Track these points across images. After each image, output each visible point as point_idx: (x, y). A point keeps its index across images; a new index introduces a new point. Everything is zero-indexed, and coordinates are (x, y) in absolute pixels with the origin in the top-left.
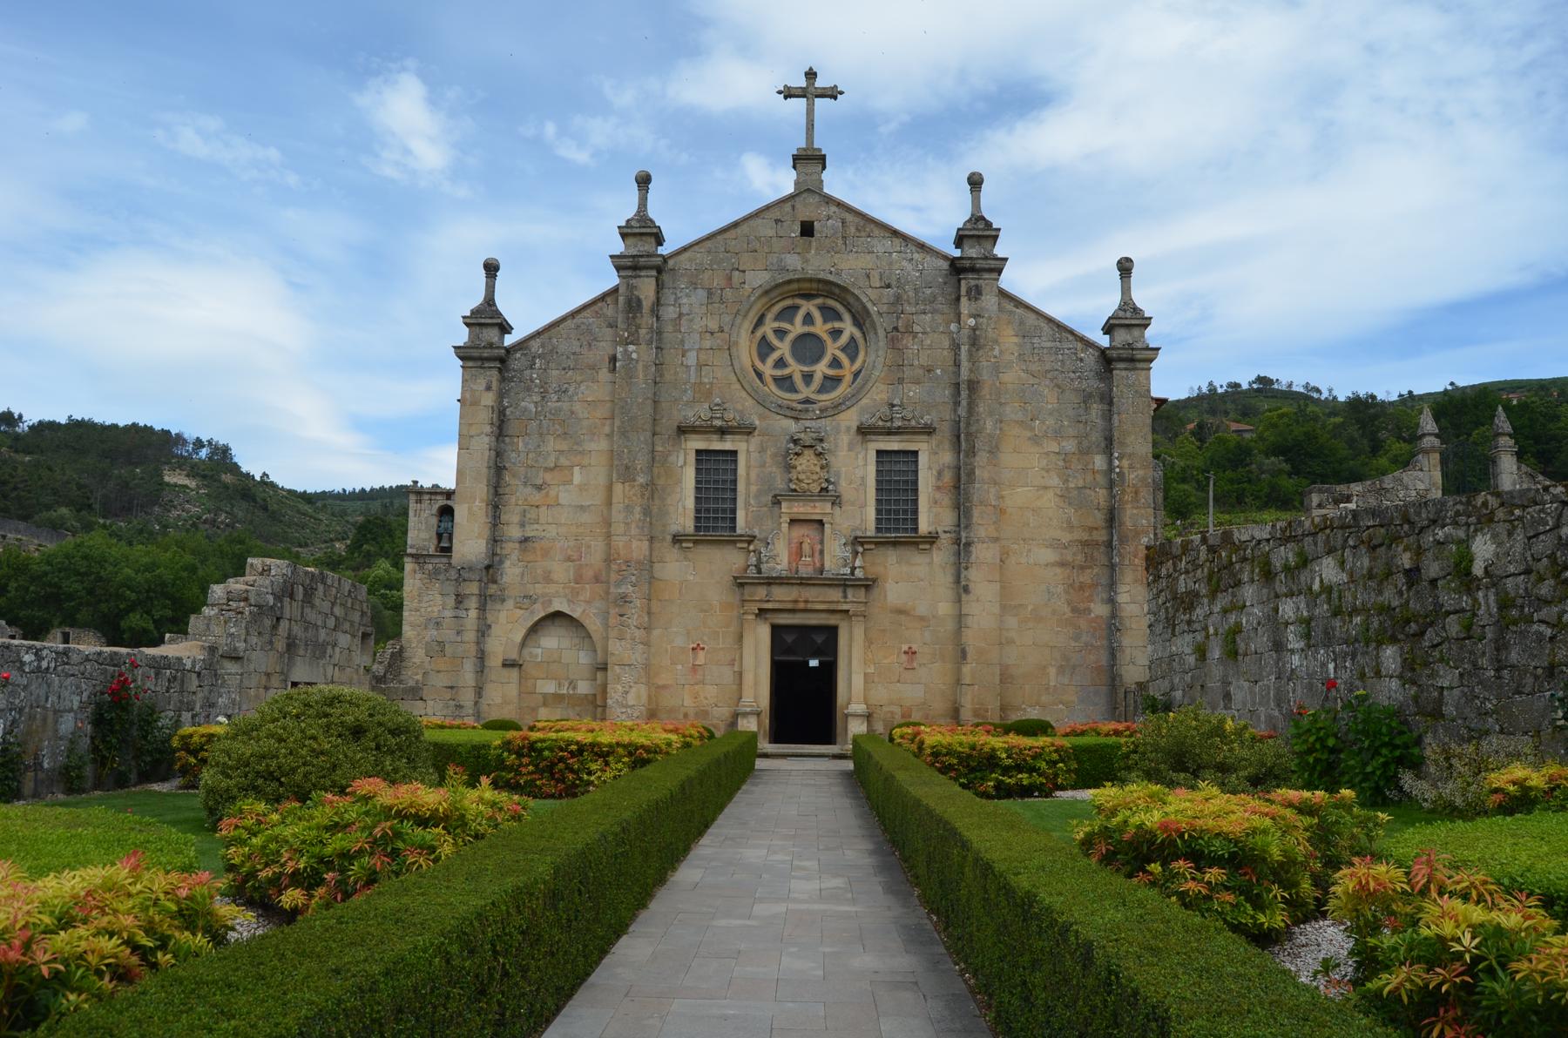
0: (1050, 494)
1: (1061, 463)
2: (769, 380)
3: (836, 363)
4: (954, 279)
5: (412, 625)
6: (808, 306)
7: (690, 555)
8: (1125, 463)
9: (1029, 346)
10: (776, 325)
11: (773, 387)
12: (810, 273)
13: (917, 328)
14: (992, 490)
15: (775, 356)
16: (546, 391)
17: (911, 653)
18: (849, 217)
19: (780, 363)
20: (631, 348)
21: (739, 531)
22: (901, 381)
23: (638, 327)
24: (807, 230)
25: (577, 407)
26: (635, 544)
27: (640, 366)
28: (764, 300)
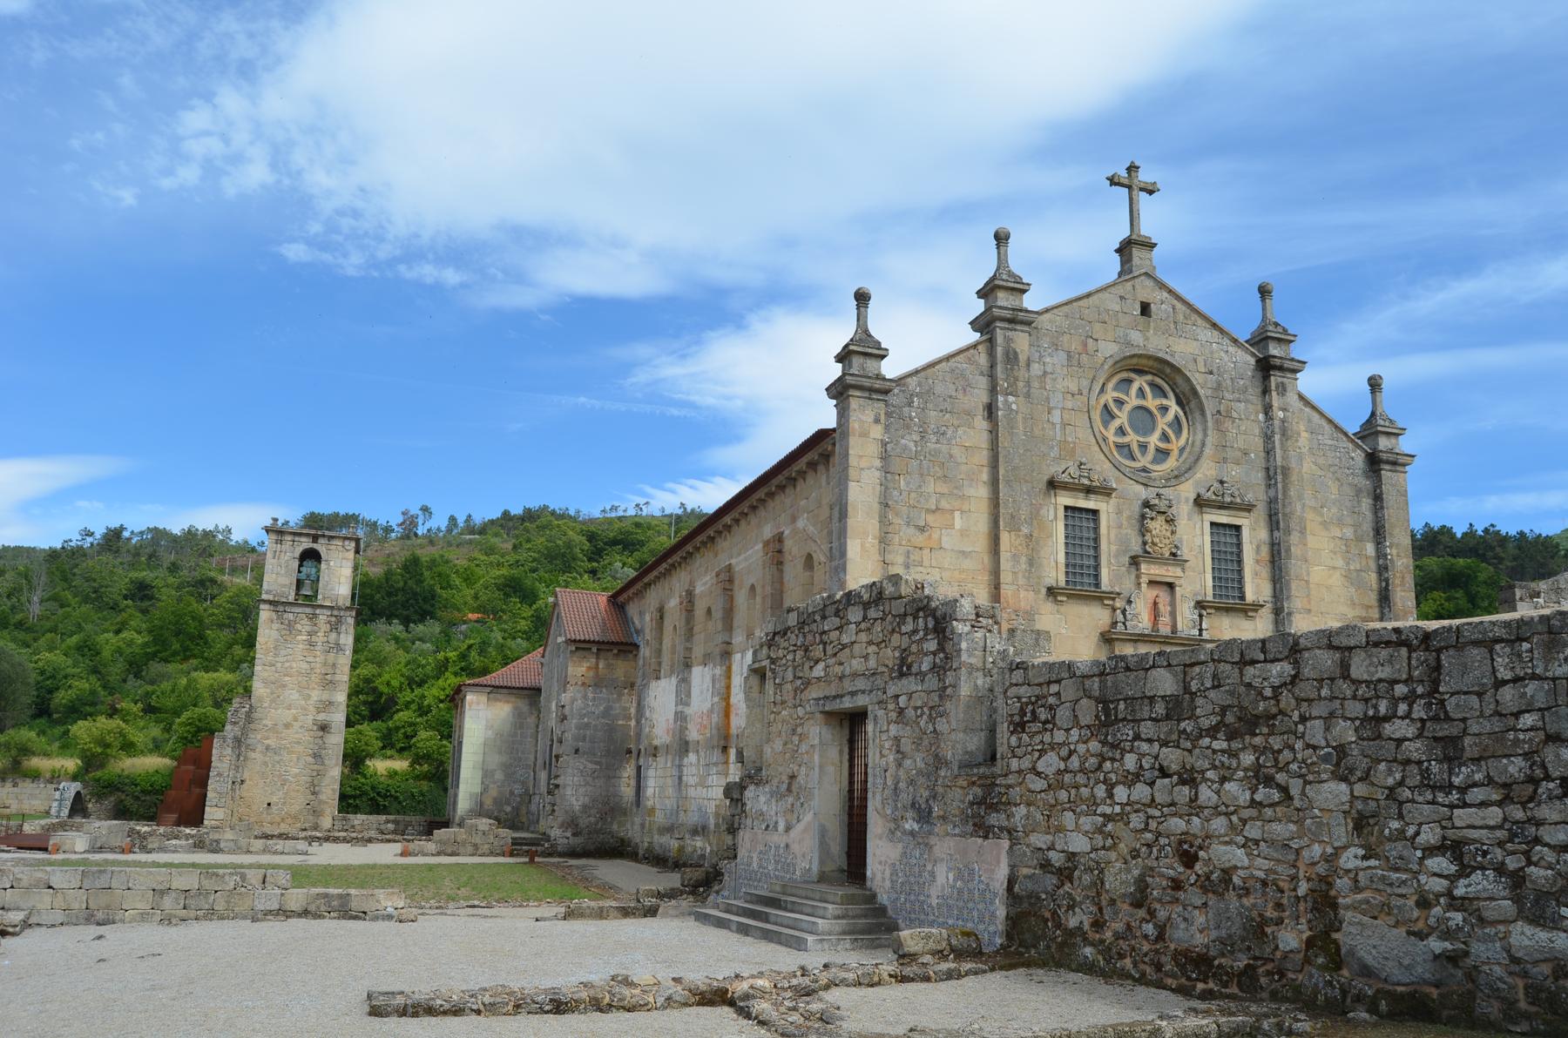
0: (1337, 574)
3: (1165, 437)
5: (265, 681)
6: (1139, 382)
7: (1063, 609)
8: (1394, 552)
10: (1116, 394)
13: (1235, 415)
15: (1116, 423)
16: (925, 432)
18: (1179, 305)
19: (1121, 431)
20: (1011, 399)
22: (1225, 460)
23: (1016, 379)
24: (1145, 309)
25: (955, 451)
26: (1023, 594)
27: (1020, 417)
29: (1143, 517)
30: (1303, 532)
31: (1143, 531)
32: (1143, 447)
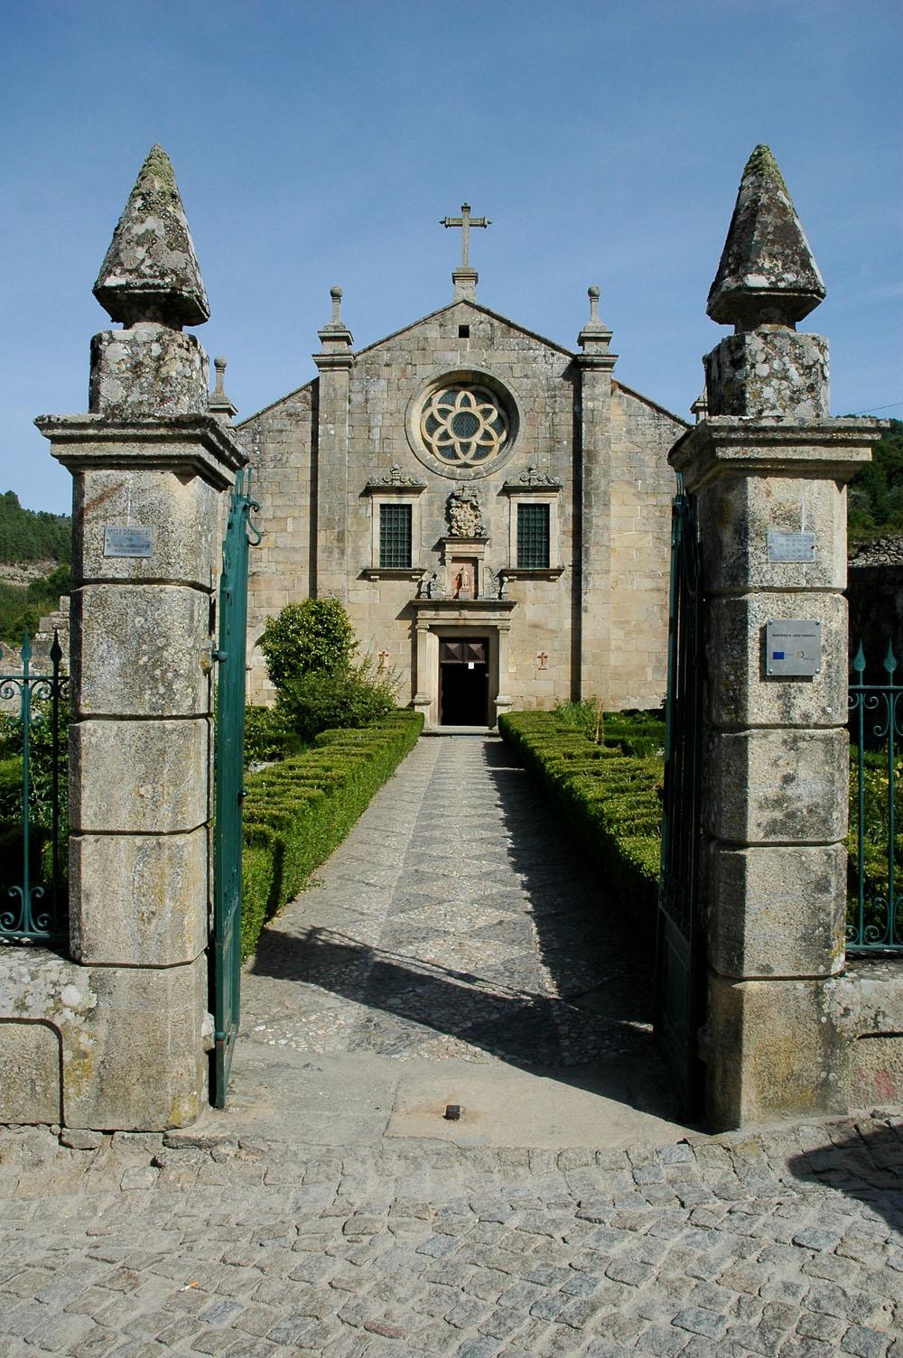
1: (658, 514)
3: (487, 436)
9: (634, 423)
11: (438, 455)
12: (466, 366)
14: (606, 534)
15: (440, 430)
18: (496, 323)
19: (445, 436)
20: (330, 426)
21: (413, 566)
24: (464, 332)
28: (432, 386)
29: (449, 507)
30: (607, 505)
31: (449, 518)
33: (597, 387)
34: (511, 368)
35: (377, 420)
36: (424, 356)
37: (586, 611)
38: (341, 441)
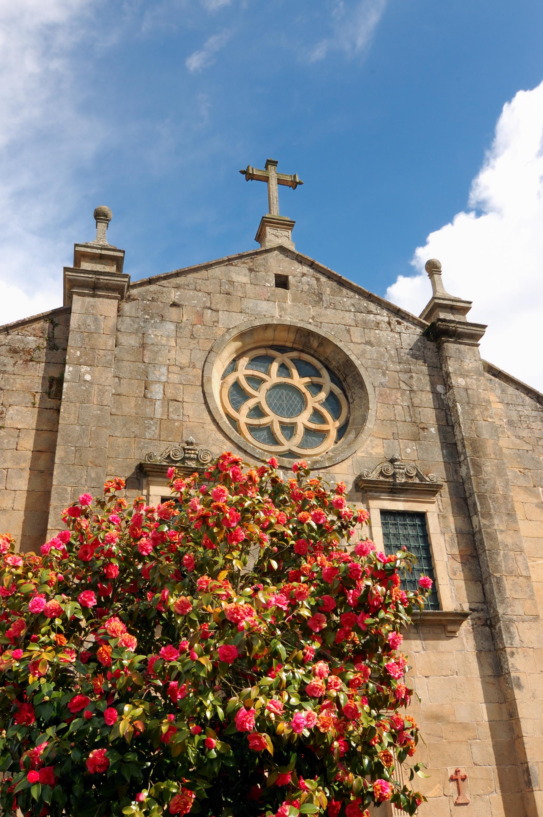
2: (244, 428)
3: (317, 416)
4: (431, 345)
12: (288, 320)
14: (519, 558)
15: (251, 403)
17: (457, 779)
19: (258, 411)
20: (84, 368)
24: (282, 282)
30: (511, 515)
32: (289, 429)
33: (460, 361)
34: (349, 331)
35: (160, 374)
36: (229, 302)
37: (519, 686)
38: (102, 392)
